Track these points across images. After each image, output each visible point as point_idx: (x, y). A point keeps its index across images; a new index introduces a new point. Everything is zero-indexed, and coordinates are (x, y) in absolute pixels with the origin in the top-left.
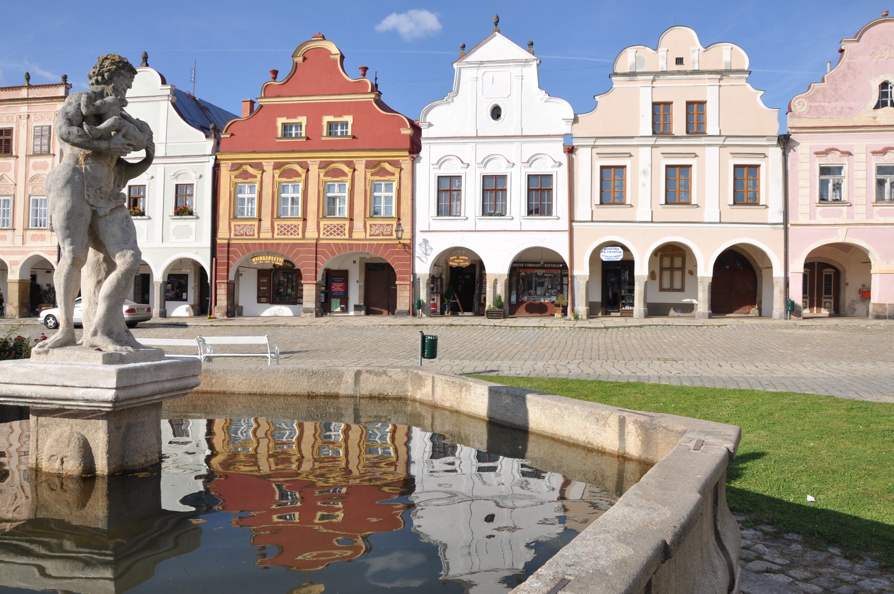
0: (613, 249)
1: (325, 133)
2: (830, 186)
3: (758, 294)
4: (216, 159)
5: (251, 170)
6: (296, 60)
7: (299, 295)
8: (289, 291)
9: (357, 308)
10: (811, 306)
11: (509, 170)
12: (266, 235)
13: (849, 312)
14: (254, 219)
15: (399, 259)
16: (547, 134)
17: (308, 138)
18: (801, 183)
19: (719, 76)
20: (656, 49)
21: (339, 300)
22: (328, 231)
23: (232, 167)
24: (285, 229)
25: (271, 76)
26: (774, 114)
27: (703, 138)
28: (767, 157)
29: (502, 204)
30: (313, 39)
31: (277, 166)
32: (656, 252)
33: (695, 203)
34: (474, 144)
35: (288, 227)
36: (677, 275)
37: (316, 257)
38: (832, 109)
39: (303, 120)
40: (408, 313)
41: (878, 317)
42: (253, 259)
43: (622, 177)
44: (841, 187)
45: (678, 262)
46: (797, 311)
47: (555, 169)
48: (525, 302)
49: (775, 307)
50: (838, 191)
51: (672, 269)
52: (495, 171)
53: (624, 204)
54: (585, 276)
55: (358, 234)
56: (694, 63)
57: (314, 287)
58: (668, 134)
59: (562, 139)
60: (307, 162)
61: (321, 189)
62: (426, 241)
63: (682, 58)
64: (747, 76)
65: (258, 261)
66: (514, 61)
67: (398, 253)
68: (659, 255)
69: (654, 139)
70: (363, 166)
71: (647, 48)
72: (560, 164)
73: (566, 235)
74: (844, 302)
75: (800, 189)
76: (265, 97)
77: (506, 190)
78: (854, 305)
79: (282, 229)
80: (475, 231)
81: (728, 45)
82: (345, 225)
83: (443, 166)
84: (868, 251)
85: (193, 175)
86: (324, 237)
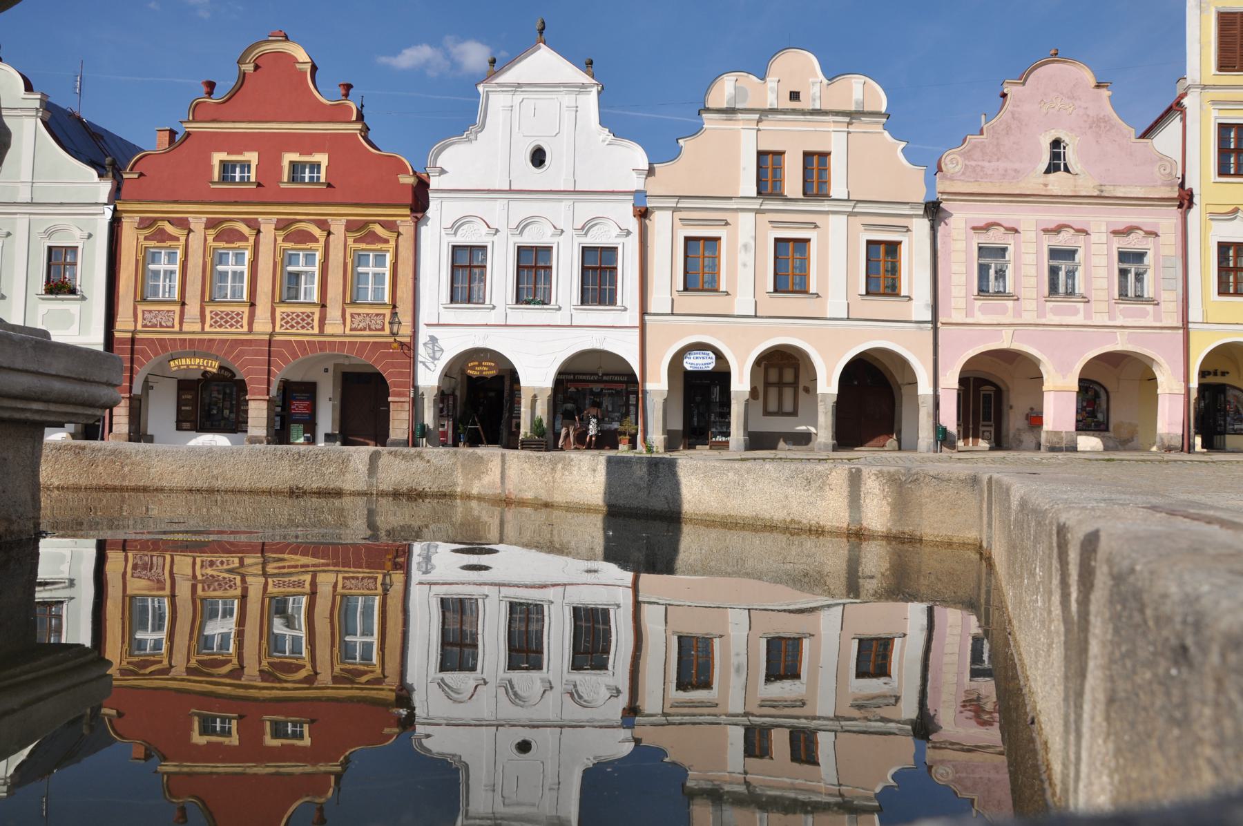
0: (700, 354)
1: (285, 178)
2: (992, 272)
4: (115, 210)
5: (170, 229)
6: (244, 67)
7: (241, 419)
8: (226, 412)
9: (329, 438)
10: (966, 437)
11: (555, 240)
12: (191, 326)
13: (1014, 445)
14: (173, 302)
15: (393, 365)
16: (611, 189)
17: (259, 185)
19: (847, 119)
20: (763, 78)
21: (301, 427)
22: (287, 323)
23: (140, 223)
24: (222, 318)
25: (204, 89)
26: (918, 173)
27: (826, 203)
29: (545, 288)
30: (270, 38)
31: (211, 224)
32: (759, 362)
33: (815, 292)
34: (506, 201)
35: (227, 314)
36: (788, 393)
37: (269, 361)
38: (993, 170)
39: (253, 157)
40: (406, 443)
41: (1052, 449)
42: (172, 363)
43: (714, 253)
45: (788, 376)
47: (621, 240)
49: (920, 436)
51: (780, 385)
52: (536, 241)
53: (716, 290)
54: (661, 391)
55: (334, 326)
56: (814, 100)
57: (264, 405)
58: (778, 195)
59: (632, 197)
60: (257, 219)
61: (279, 259)
62: (433, 339)
63: (799, 93)
64: (885, 120)
65: (179, 366)
66: (565, 85)
67: (392, 355)
69: (760, 201)
70: (343, 228)
71: (750, 76)
72: (628, 233)
74: (1008, 430)
76: (194, 121)
77: (550, 268)
78: (1020, 435)
79: (218, 318)
80: (506, 325)
81: (859, 78)
82: (313, 313)
84: (1039, 360)
85: (77, 233)
86: (282, 331)
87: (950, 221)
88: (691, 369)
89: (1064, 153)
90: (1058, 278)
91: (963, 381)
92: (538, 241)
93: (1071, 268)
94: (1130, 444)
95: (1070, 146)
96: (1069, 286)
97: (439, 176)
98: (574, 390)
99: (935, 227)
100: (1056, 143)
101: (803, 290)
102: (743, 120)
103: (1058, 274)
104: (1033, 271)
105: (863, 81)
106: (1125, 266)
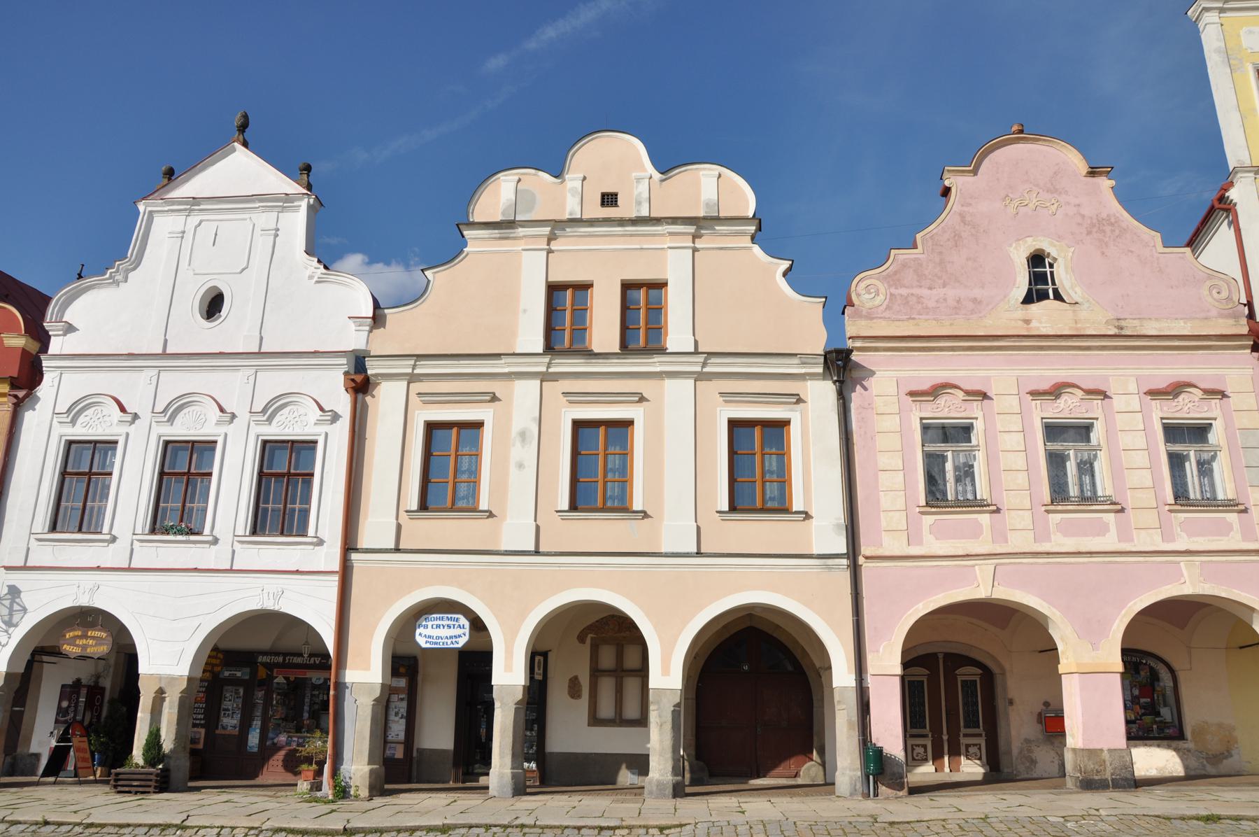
3: (815, 729)
10: (937, 757)
11: (222, 430)
13: (1021, 768)
18: (884, 461)
19: (692, 229)
20: (558, 173)
26: (814, 307)
27: (657, 359)
28: (804, 402)
34: (155, 371)
41: (1089, 784)
44: (973, 472)
46: (894, 774)
48: (280, 749)
49: (839, 764)
50: (968, 480)
53: (475, 510)
56: (639, 203)
63: (616, 195)
68: (588, 641)
69: (546, 359)
71: (541, 173)
72: (335, 417)
73: (333, 583)
74: (1009, 744)
75: (882, 476)
78: (1030, 751)
81: (710, 169)
83: (81, 419)
84: (1045, 617)
87: (872, 383)
88: (428, 646)
89: (1052, 273)
90: (1066, 474)
91: (910, 661)
92: (192, 432)
93: (1086, 457)
94: (1225, 761)
95: (1060, 260)
96: (1088, 487)
97: (65, 335)
98: (283, 681)
99: (845, 393)
100: (1037, 259)
101: (621, 506)
102: (525, 236)
103: (1065, 467)
104: (1019, 461)
105: (717, 173)
106: (1177, 448)
